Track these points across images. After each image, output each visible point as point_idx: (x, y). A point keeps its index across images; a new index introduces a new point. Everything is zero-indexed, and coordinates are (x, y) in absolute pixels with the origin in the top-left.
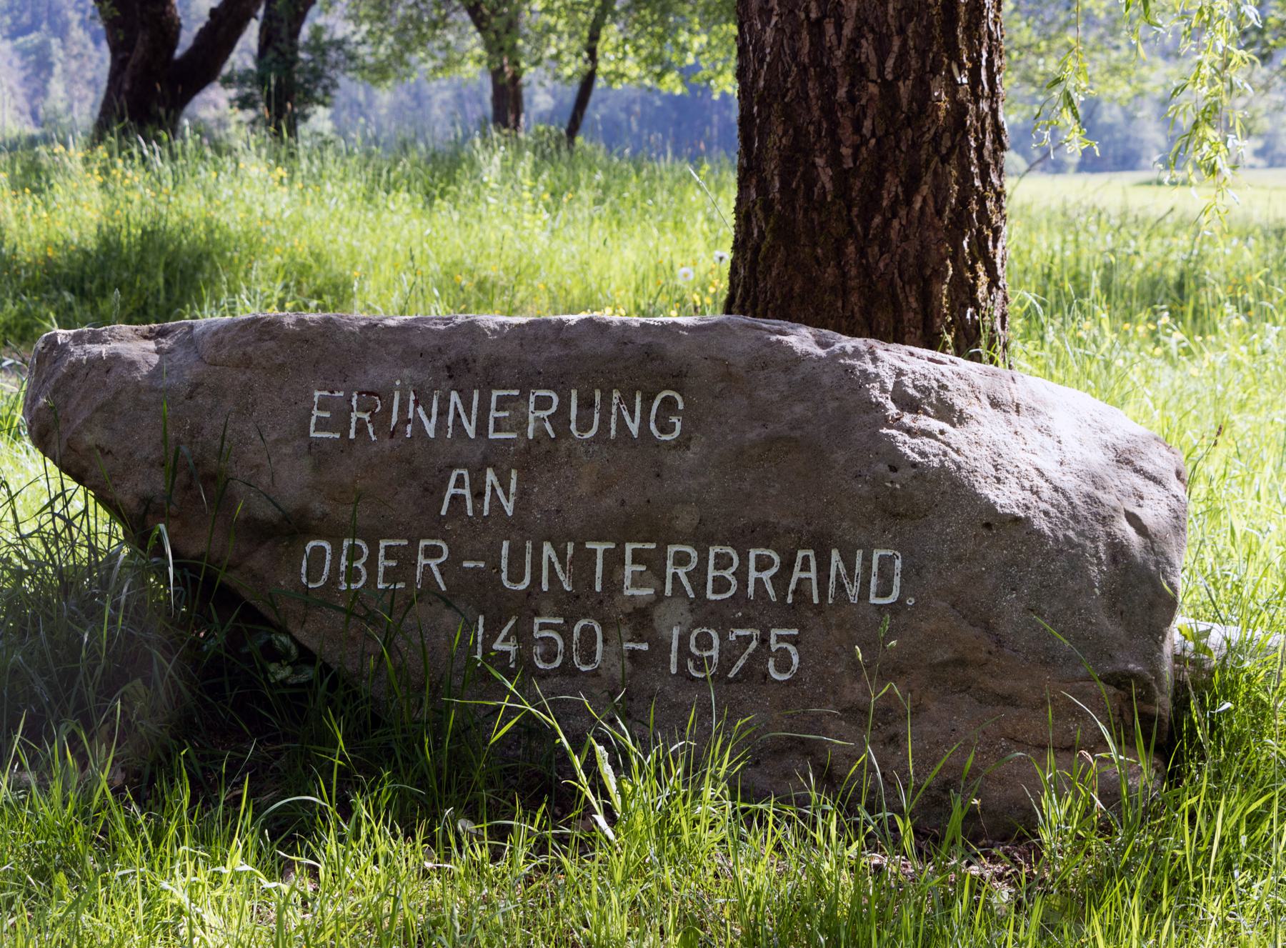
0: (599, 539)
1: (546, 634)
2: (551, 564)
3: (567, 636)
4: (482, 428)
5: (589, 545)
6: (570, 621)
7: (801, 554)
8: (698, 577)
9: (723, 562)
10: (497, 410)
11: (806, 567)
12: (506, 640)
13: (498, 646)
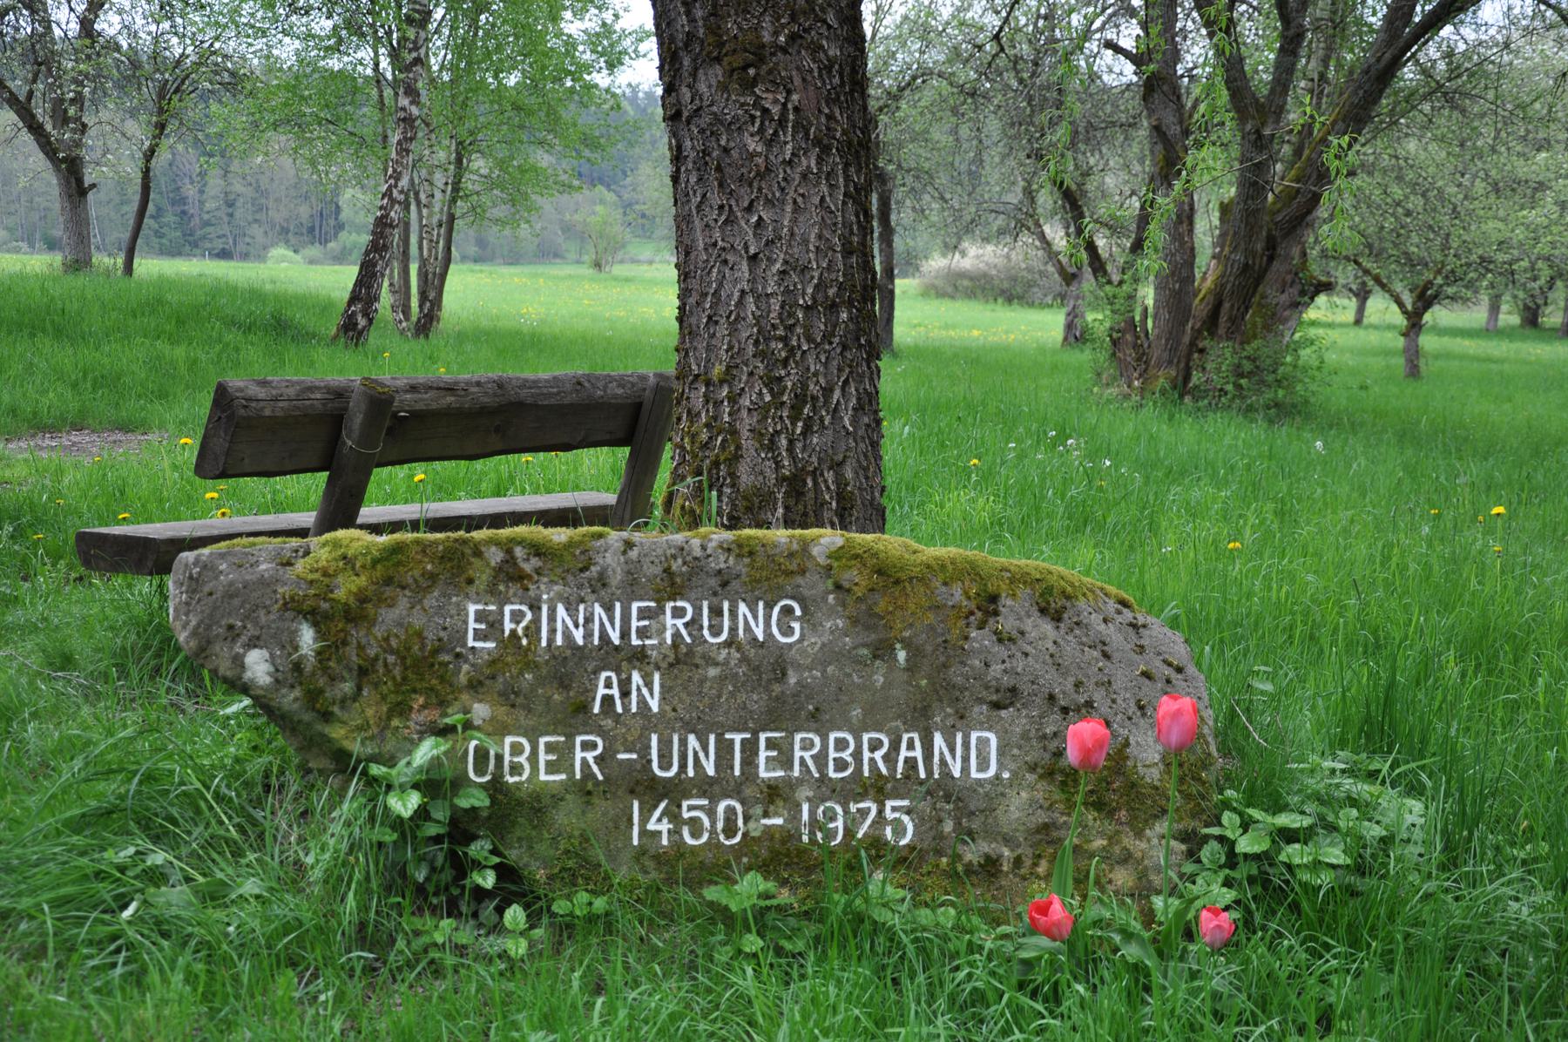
0: (738, 731)
1: (694, 814)
2: (696, 753)
3: (711, 813)
4: (625, 634)
5: (728, 736)
6: (714, 801)
7: (905, 737)
8: (820, 759)
9: (841, 745)
10: (639, 619)
11: (911, 746)
12: (659, 820)
13: (651, 826)
